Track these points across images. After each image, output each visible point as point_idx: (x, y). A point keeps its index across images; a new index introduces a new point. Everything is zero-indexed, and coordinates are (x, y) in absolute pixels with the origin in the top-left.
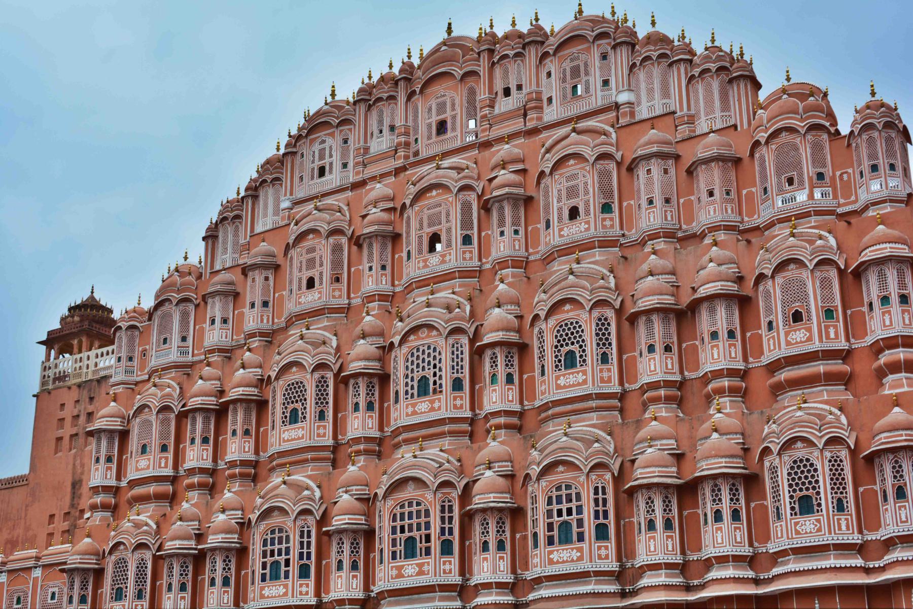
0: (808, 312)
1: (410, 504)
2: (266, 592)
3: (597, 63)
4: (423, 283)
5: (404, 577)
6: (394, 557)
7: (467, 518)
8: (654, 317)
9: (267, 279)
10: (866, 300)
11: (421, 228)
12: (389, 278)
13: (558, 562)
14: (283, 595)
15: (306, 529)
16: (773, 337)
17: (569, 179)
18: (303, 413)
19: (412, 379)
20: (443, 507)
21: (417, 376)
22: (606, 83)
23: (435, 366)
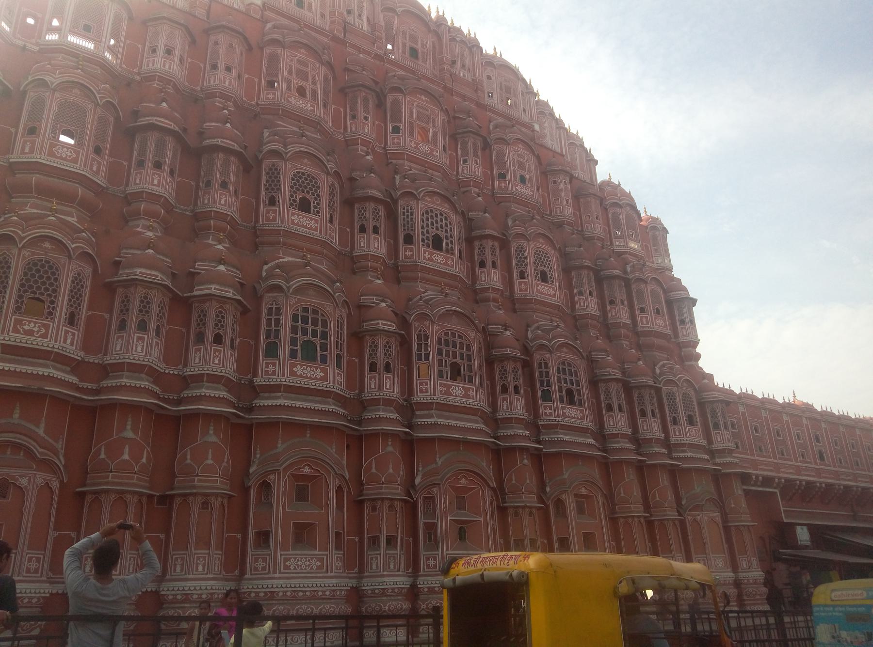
0: (663, 311)
1: (454, 335)
2: (298, 370)
4: (412, 159)
6: (441, 375)
8: (592, 274)
10: (677, 317)
11: (411, 116)
13: (569, 417)
16: (646, 318)
17: (518, 155)
18: (315, 207)
21: (433, 232)
22: (524, 110)
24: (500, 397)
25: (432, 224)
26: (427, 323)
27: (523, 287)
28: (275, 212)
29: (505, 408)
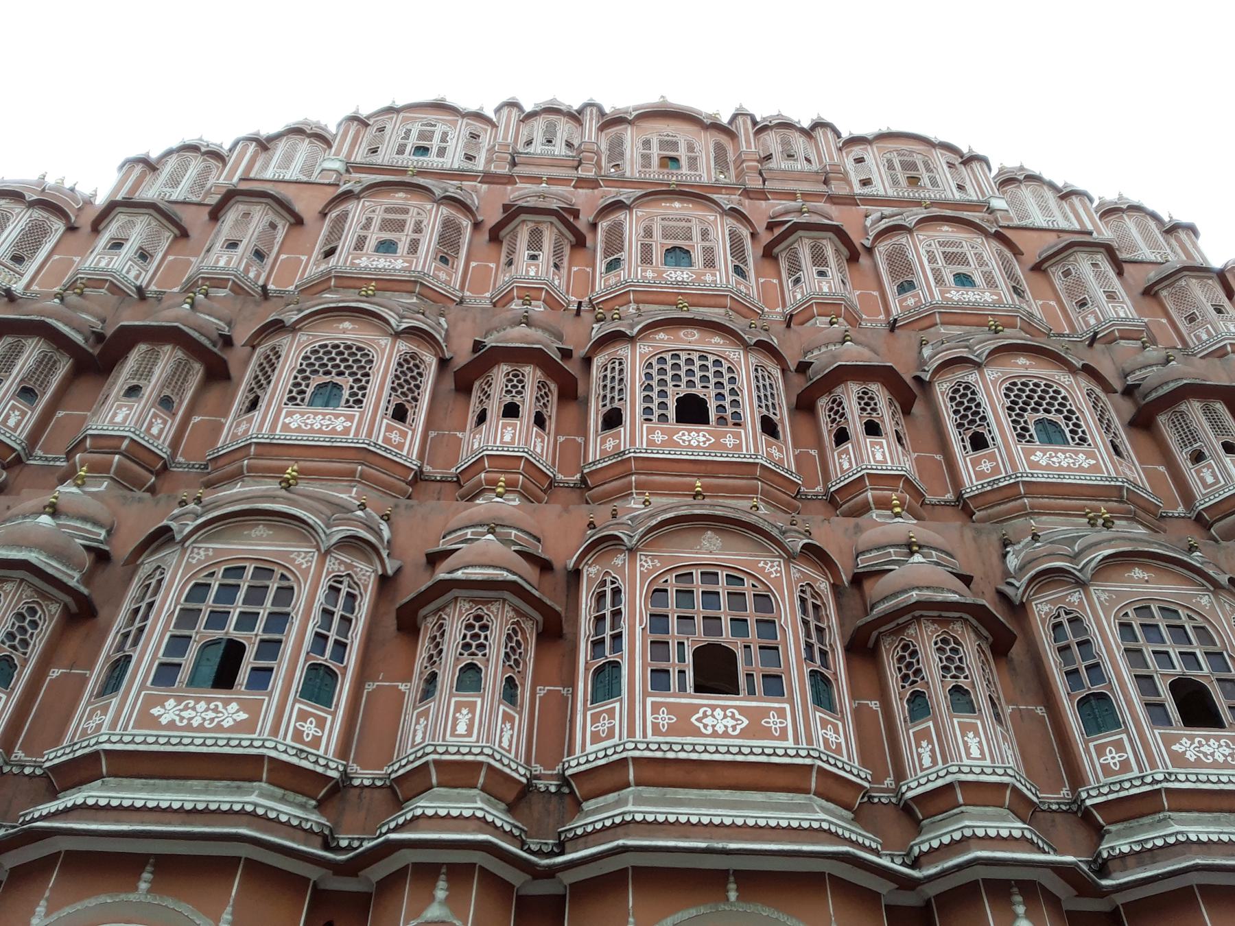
1: (710, 576)
2: (168, 712)
3: (945, 167)
5: (697, 732)
6: (660, 679)
7: (862, 648)
9: (273, 226)
11: (648, 232)
12: (563, 288)
14: (230, 729)
15: (344, 589)
18: (351, 395)
19: (662, 393)
20: (803, 601)
23: (719, 385)
24: (907, 734)
25: (676, 377)
26: (619, 560)
27: (986, 466)
28: (250, 421)
29: (927, 761)
